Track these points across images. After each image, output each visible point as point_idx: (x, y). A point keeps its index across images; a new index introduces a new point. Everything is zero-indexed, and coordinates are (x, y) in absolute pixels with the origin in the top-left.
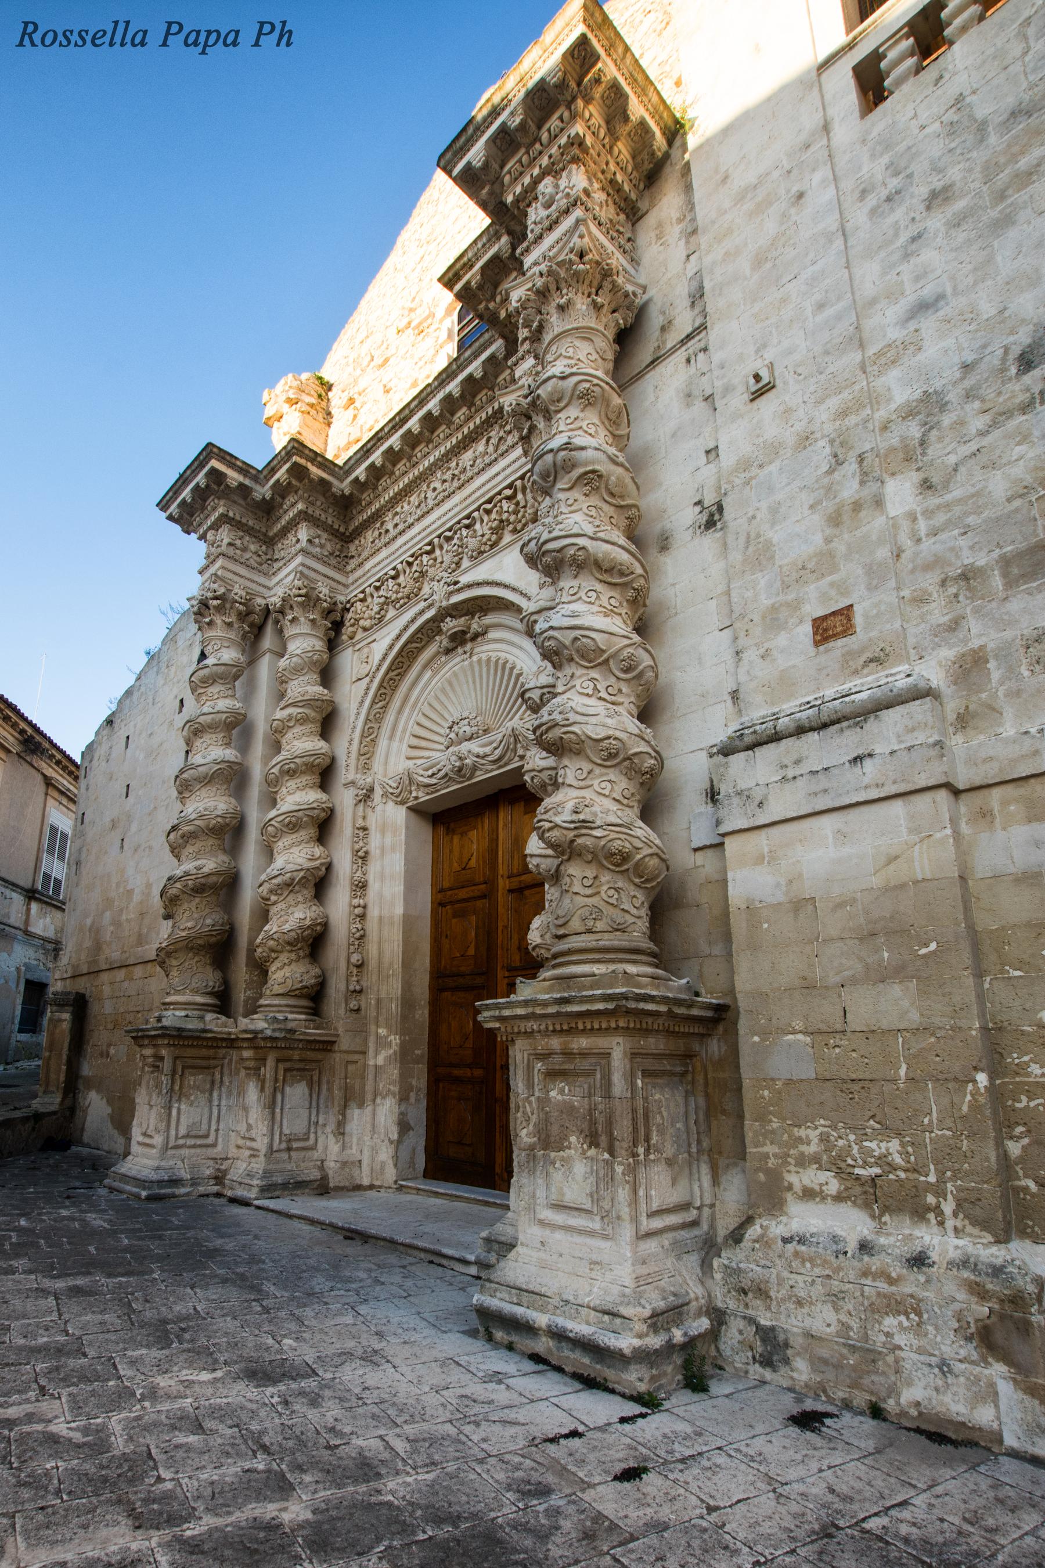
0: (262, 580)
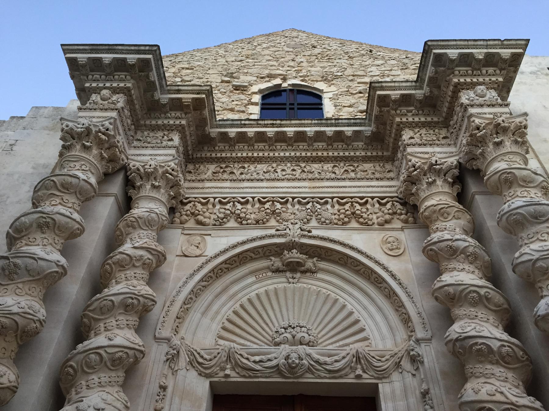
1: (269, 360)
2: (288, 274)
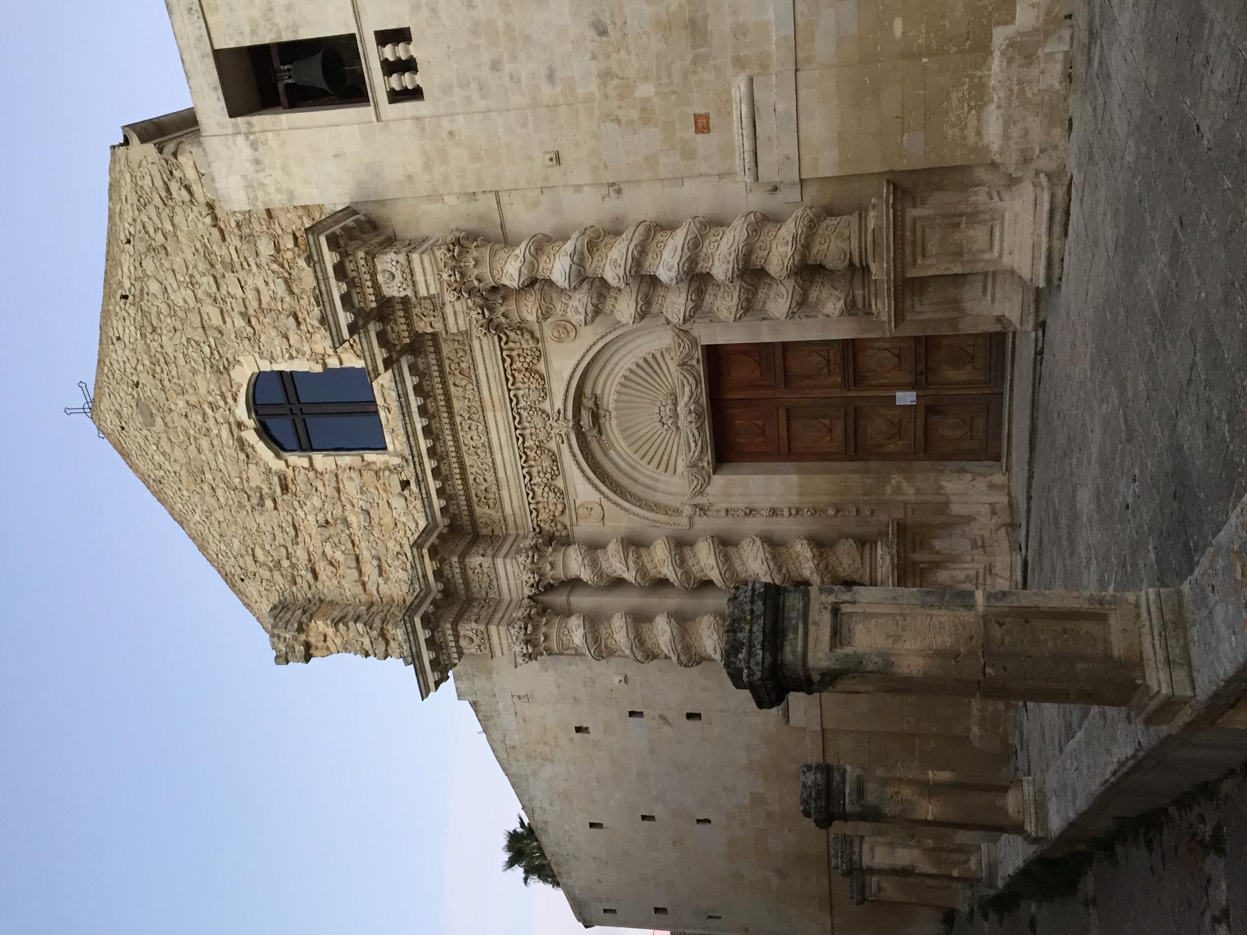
0: (504, 605)
2: (602, 421)
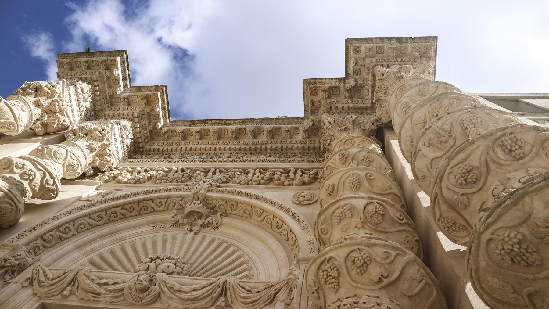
1: (116, 283)
